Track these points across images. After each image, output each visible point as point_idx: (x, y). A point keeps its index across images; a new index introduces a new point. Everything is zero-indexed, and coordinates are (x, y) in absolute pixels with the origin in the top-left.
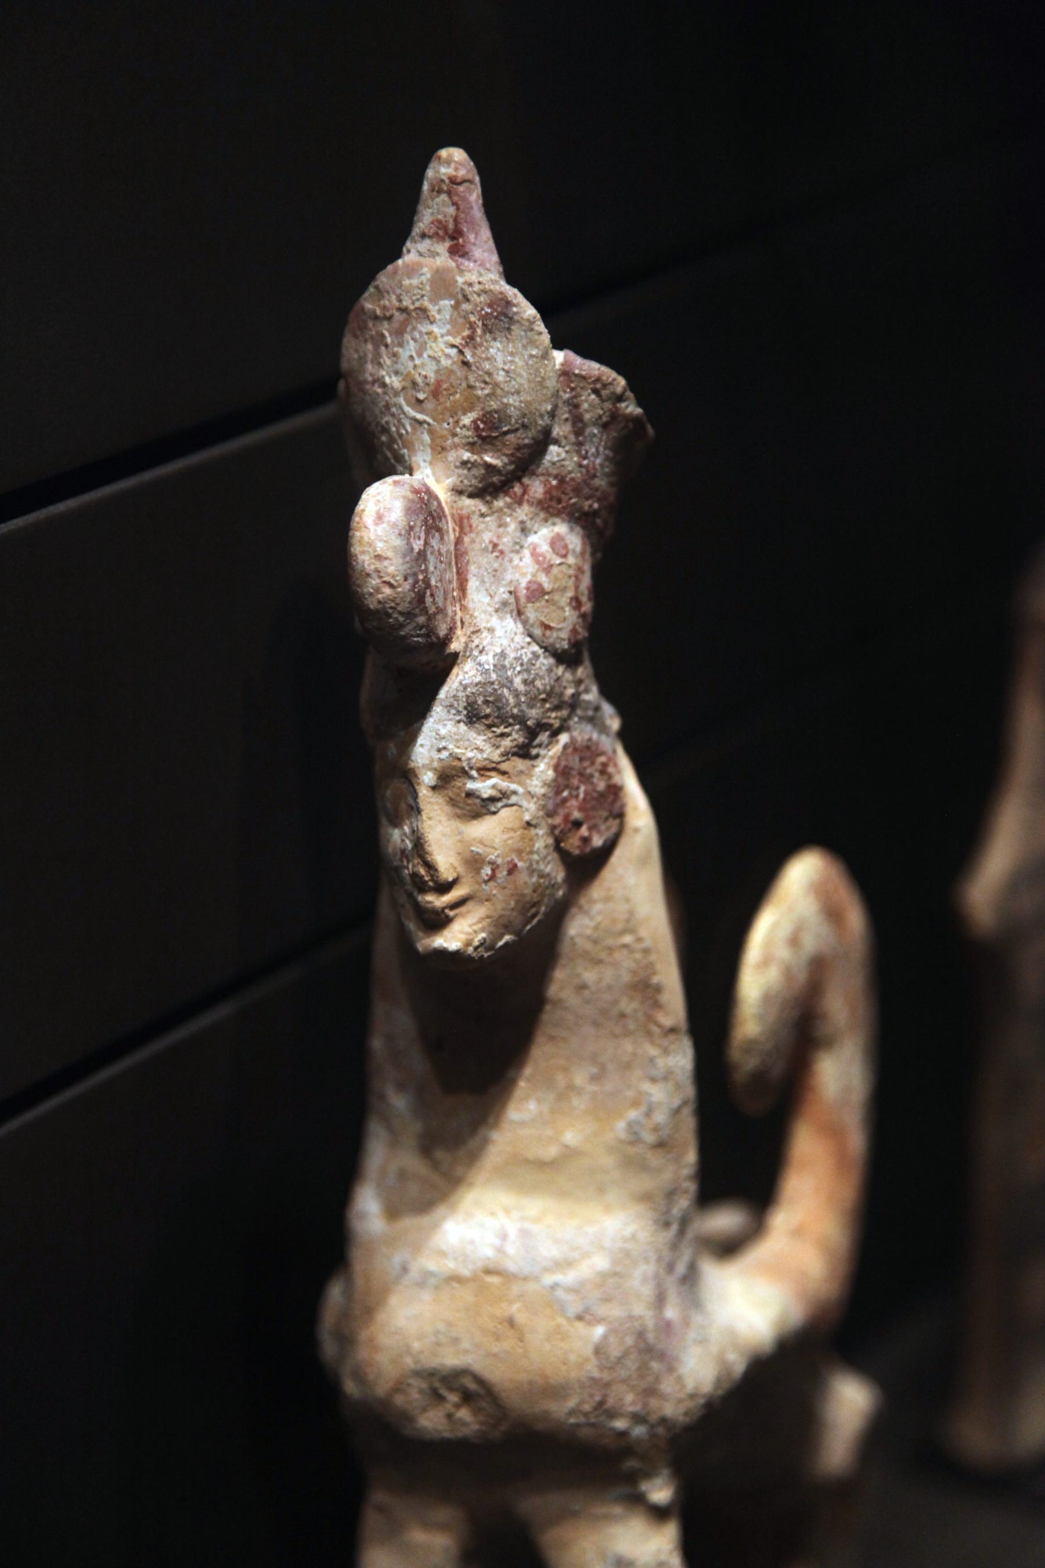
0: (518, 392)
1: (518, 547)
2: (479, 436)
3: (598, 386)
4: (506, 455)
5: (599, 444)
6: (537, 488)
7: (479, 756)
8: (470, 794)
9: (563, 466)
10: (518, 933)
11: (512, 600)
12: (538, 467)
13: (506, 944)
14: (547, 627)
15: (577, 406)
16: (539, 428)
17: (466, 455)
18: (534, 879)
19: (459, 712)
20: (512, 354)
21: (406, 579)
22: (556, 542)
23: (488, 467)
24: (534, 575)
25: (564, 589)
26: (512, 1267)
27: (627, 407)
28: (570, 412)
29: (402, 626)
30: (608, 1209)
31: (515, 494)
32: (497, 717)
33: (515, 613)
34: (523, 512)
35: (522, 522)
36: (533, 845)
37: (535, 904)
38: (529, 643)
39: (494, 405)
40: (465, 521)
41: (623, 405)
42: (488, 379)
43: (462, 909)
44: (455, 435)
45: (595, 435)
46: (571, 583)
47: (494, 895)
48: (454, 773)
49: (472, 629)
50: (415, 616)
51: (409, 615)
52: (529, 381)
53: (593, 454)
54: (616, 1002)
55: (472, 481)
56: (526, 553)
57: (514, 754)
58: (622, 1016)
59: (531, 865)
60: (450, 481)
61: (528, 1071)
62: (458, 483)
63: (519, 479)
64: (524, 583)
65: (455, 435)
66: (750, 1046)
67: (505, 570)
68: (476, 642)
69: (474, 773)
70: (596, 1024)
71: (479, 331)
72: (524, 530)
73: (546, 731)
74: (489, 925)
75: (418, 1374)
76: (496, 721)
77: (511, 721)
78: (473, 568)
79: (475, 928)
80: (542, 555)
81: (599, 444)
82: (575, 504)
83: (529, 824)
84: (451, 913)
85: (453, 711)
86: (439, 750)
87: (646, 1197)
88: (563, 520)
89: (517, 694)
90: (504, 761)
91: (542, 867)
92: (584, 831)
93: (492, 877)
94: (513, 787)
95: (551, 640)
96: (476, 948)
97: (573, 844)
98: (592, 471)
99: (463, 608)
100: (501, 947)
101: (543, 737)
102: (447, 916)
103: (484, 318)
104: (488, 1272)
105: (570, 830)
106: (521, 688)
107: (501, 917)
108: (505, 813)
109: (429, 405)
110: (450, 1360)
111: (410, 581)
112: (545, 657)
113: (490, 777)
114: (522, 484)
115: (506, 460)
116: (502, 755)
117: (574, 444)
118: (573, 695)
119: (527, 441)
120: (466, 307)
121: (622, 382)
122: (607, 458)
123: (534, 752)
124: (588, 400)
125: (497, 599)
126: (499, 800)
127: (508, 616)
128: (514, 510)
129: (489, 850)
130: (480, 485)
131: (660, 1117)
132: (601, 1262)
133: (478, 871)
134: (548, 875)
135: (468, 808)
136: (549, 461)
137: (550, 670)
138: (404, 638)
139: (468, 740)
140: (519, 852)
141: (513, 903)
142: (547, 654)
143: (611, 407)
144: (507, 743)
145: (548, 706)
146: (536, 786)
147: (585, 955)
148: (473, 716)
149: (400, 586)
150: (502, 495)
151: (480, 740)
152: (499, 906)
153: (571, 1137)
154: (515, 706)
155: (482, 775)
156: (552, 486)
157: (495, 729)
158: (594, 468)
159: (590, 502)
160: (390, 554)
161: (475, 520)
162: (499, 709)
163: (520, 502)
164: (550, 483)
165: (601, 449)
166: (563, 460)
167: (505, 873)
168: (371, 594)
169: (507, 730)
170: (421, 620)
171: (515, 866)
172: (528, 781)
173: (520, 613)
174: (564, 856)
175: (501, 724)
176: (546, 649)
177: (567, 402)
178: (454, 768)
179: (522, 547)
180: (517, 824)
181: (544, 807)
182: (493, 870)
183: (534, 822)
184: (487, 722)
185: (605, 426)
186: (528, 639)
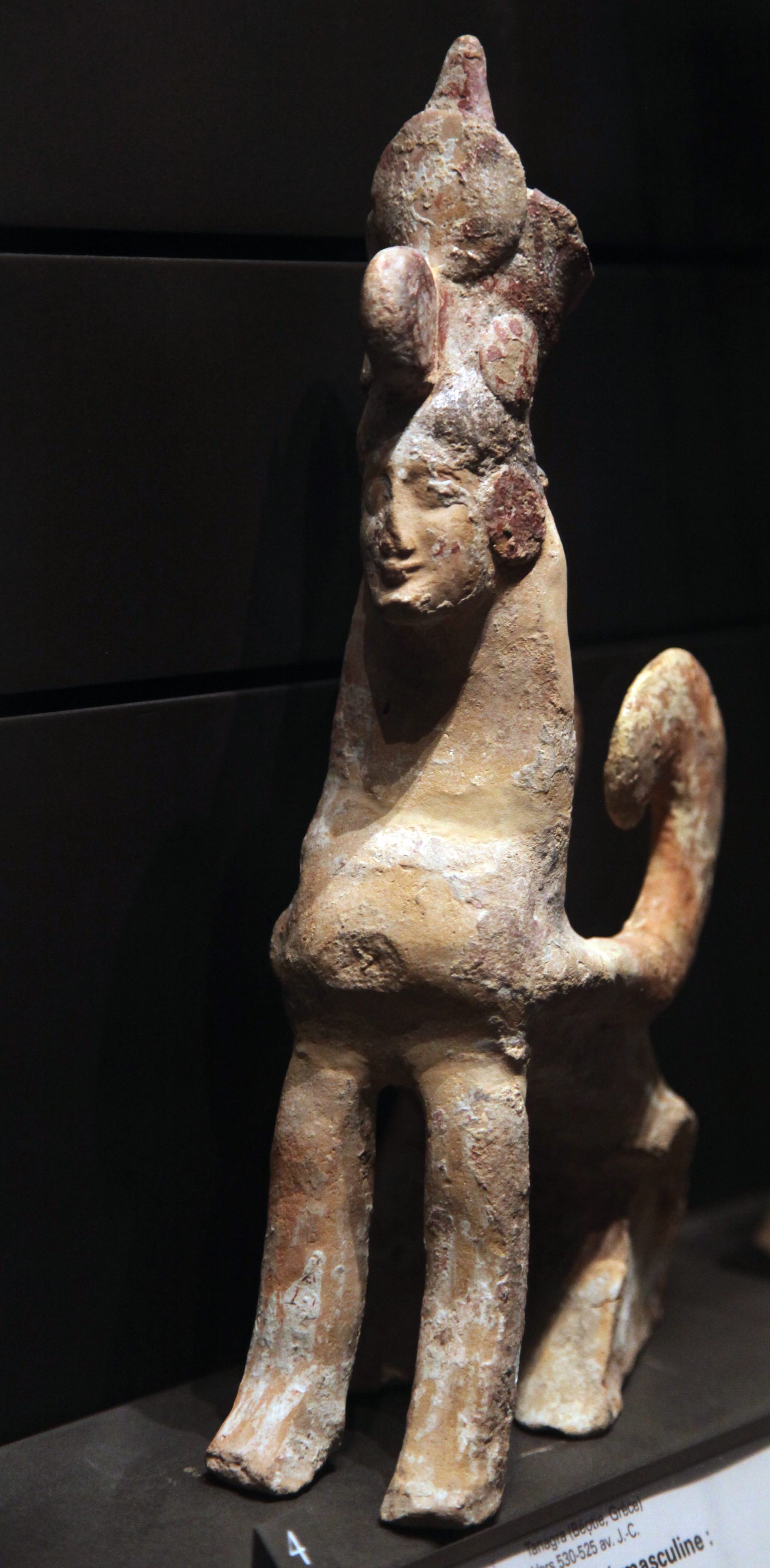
0: (497, 207)
1: (485, 323)
2: (466, 236)
3: (556, 217)
4: (484, 253)
5: (553, 262)
6: (504, 283)
7: (440, 462)
8: (430, 489)
9: (525, 271)
10: (455, 601)
11: (477, 358)
12: (507, 267)
13: (445, 607)
14: (501, 381)
15: (539, 229)
16: (510, 236)
17: (455, 249)
18: (471, 563)
19: (429, 428)
20: (496, 179)
21: (401, 309)
22: (512, 324)
23: (470, 259)
24: (495, 343)
25: (517, 358)
26: (422, 863)
27: (576, 239)
28: (534, 232)
29: (394, 344)
30: (500, 834)
31: (488, 284)
32: (457, 436)
33: (478, 367)
34: (492, 299)
35: (490, 306)
36: (473, 537)
37: (469, 583)
38: (486, 391)
39: (479, 214)
40: (449, 297)
41: (574, 236)
42: (476, 195)
43: (416, 574)
44: (448, 234)
45: (550, 254)
46: (522, 355)
47: (440, 566)
48: (420, 471)
49: (445, 372)
50: (405, 339)
51: (401, 337)
52: (506, 200)
53: (547, 268)
54: (523, 682)
55: (457, 269)
56: (491, 327)
57: (466, 467)
58: (527, 693)
59: (469, 551)
60: (442, 267)
61: (451, 728)
62: (447, 269)
63: (492, 274)
64: (487, 346)
65: (448, 234)
66: (619, 765)
67: (474, 337)
68: (447, 381)
69: (435, 473)
70: (506, 697)
71: (474, 161)
72: (491, 311)
73: (492, 457)
74: (435, 588)
75: (341, 937)
76: (456, 438)
77: (466, 441)
78: (451, 331)
79: (423, 588)
80: (503, 330)
81: (553, 262)
82: (530, 302)
83: (471, 520)
84: (407, 575)
85: (425, 427)
86: (412, 453)
87: (529, 830)
88: (521, 312)
89: (473, 423)
90: (458, 470)
91: (478, 556)
93: (440, 553)
94: (463, 490)
95: (502, 392)
96: (423, 603)
97: (503, 547)
98: (546, 281)
99: (441, 356)
100: (441, 609)
101: (489, 461)
102: (404, 577)
103: (478, 152)
104: (404, 866)
105: (501, 537)
106: (478, 420)
107: (443, 584)
108: (454, 507)
109: (432, 212)
110: (369, 927)
111: (404, 312)
112: (497, 404)
113: (447, 479)
114: (493, 278)
115: (483, 256)
116: (458, 464)
117: (534, 256)
118: (515, 439)
119: (500, 244)
120: (467, 143)
121: (573, 219)
122: (557, 275)
123: (481, 470)
124: (548, 226)
125: (466, 355)
127: (473, 368)
128: (485, 296)
129: (441, 532)
130: (463, 274)
131: (546, 772)
132: (490, 868)
133: (430, 546)
134: (481, 564)
135: (428, 499)
136: (515, 265)
137: (499, 414)
138: (395, 354)
139: (433, 449)
140: (463, 538)
141: (453, 576)
142: (498, 401)
143: (564, 235)
144: (461, 457)
145: (495, 438)
146: (480, 495)
147: (504, 642)
148: (439, 433)
149: (396, 313)
150: (478, 284)
151: (442, 451)
152: (443, 575)
154: (471, 431)
155: (441, 476)
156: (515, 284)
157: (454, 445)
158: (548, 278)
159: (542, 304)
160: (391, 288)
161: (457, 298)
162: (459, 430)
163: (490, 291)
164: (514, 281)
165: (554, 266)
166: (526, 266)
167: (450, 551)
168: (374, 316)
169: (464, 447)
170: (409, 343)
171: (458, 548)
172: (474, 490)
173: (482, 368)
174: (495, 555)
175: (459, 442)
176: (498, 397)
177: (532, 224)
178: (421, 468)
179: (488, 323)
180: (463, 517)
181: (484, 512)
182: (441, 547)
183: (475, 520)
184: (449, 438)
185: (558, 249)
186: (486, 388)
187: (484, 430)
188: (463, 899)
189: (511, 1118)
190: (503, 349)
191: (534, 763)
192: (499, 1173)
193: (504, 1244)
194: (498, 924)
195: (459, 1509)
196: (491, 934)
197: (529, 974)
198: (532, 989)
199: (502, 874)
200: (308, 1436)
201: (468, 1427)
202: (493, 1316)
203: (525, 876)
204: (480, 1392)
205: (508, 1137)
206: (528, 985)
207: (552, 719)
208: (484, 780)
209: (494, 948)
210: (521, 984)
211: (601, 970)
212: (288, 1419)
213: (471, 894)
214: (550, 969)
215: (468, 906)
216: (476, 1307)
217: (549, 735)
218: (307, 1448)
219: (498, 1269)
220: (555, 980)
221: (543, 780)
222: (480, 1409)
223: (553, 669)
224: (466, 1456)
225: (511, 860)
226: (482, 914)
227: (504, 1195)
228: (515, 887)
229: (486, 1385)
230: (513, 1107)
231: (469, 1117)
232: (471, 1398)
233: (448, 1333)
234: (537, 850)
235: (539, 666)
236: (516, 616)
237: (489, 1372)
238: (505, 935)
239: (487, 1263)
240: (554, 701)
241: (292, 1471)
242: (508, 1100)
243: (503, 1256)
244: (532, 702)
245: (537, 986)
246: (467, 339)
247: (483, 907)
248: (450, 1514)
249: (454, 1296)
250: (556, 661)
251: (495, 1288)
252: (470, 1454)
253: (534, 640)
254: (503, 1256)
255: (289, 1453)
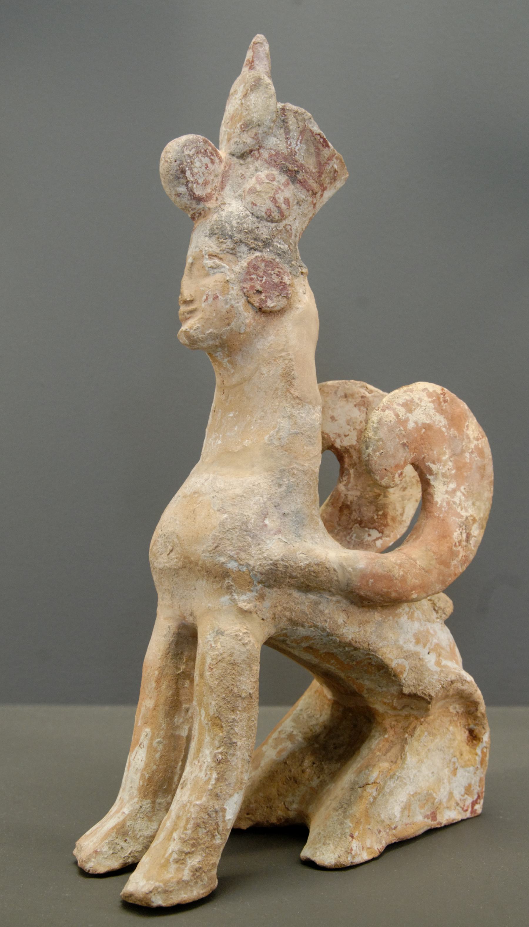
0: (257, 112)
20: (258, 98)
24: (255, 185)
34: (258, 164)
40: (232, 165)
46: (273, 192)
52: (262, 107)
67: (244, 184)
72: (257, 170)
78: (230, 182)
80: (261, 179)
87: (270, 469)
89: (232, 227)
92: (263, 296)
94: (223, 264)
106: (236, 225)
111: (178, 162)
125: (237, 194)
126: (216, 268)
132: (239, 491)
144: (224, 246)
153: (246, 443)
160: (171, 151)
162: (222, 231)
163: (257, 159)
167: (212, 299)
171: (218, 297)
187: (240, 231)
188: (216, 509)
189: (237, 647)
190: (258, 188)
191: (277, 429)
192: (222, 681)
193: (222, 727)
194: (233, 523)
195: (147, 894)
196: (227, 529)
197: (253, 555)
198: (254, 565)
199: (244, 494)
200: (126, 841)
201: (175, 842)
202: (209, 773)
203: (262, 497)
204: (188, 821)
205: (232, 658)
206: (252, 563)
207: (290, 402)
208: (250, 442)
209: (227, 537)
210: (246, 561)
211: (323, 561)
212: (113, 828)
213: (221, 506)
214: (269, 553)
215: (218, 513)
216: (201, 766)
217: (286, 411)
218: (122, 848)
219: (217, 743)
220: (271, 560)
221: (280, 439)
222: (185, 832)
223: (292, 373)
224: (168, 860)
225: (254, 487)
226: (225, 516)
227: (224, 695)
228: (252, 503)
229: (193, 816)
230: (240, 640)
231: (211, 645)
232: (182, 823)
233: (186, 782)
234: (275, 482)
235: (285, 372)
236: (272, 343)
237: (197, 808)
238: (236, 530)
239: (211, 738)
240: (292, 392)
241: (104, 860)
242: (236, 635)
243: (221, 734)
244: (280, 394)
245: (259, 563)
246: (239, 185)
247: (226, 513)
248: (141, 896)
249: (194, 759)
250: (295, 368)
251: (213, 754)
252: (171, 860)
253: (282, 357)
254: (221, 734)
255: (105, 849)
